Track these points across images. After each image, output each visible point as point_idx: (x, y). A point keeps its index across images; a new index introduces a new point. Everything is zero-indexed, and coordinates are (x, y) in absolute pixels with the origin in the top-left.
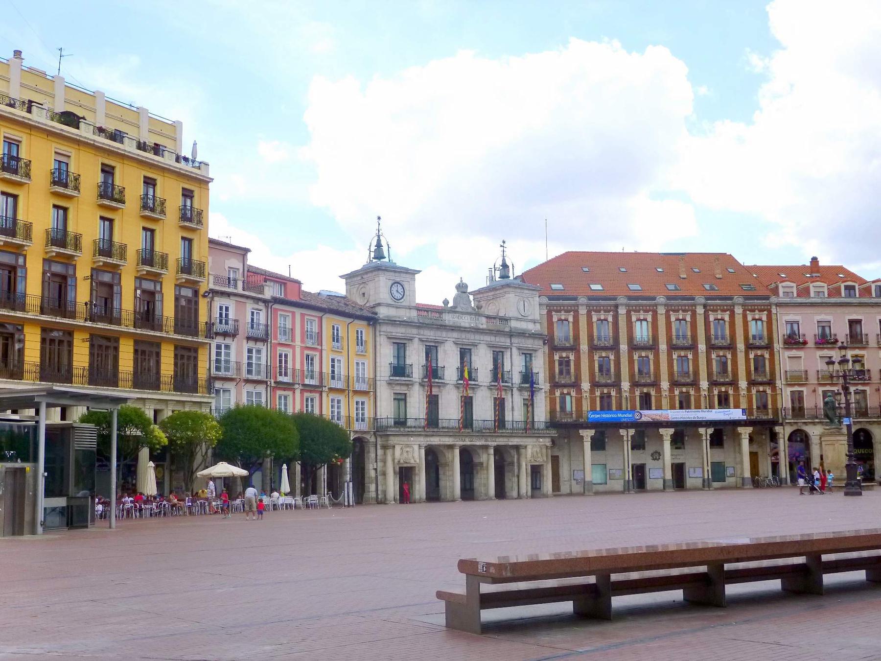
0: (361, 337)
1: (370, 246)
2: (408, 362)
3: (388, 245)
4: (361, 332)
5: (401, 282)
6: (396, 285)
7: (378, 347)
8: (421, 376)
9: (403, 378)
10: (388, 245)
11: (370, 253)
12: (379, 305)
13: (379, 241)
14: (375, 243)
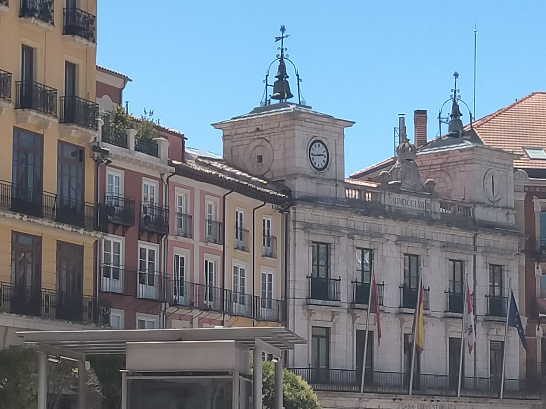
0: (268, 231)
1: (267, 76)
2: (333, 275)
3: (298, 75)
4: (268, 221)
5: (324, 141)
6: (317, 144)
7: (291, 249)
8: (351, 300)
9: (328, 302)
10: (298, 75)
11: (266, 88)
12: (294, 176)
13: (282, 68)
14: (275, 71)
